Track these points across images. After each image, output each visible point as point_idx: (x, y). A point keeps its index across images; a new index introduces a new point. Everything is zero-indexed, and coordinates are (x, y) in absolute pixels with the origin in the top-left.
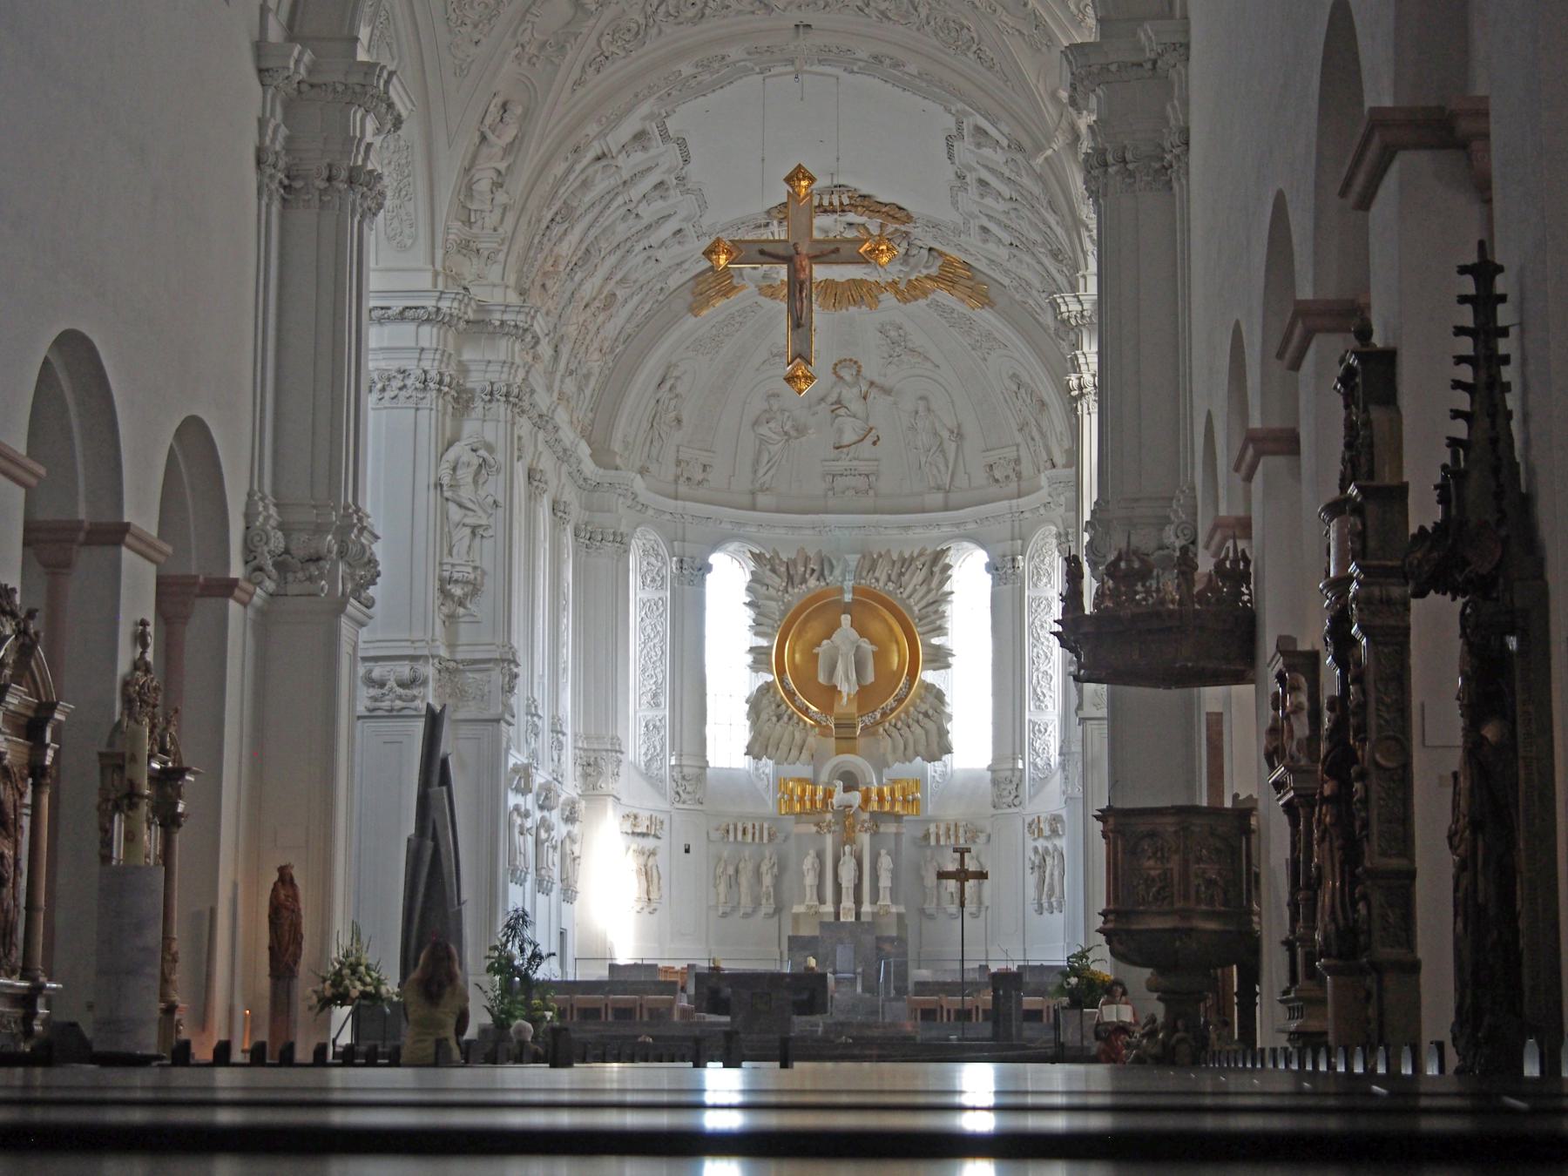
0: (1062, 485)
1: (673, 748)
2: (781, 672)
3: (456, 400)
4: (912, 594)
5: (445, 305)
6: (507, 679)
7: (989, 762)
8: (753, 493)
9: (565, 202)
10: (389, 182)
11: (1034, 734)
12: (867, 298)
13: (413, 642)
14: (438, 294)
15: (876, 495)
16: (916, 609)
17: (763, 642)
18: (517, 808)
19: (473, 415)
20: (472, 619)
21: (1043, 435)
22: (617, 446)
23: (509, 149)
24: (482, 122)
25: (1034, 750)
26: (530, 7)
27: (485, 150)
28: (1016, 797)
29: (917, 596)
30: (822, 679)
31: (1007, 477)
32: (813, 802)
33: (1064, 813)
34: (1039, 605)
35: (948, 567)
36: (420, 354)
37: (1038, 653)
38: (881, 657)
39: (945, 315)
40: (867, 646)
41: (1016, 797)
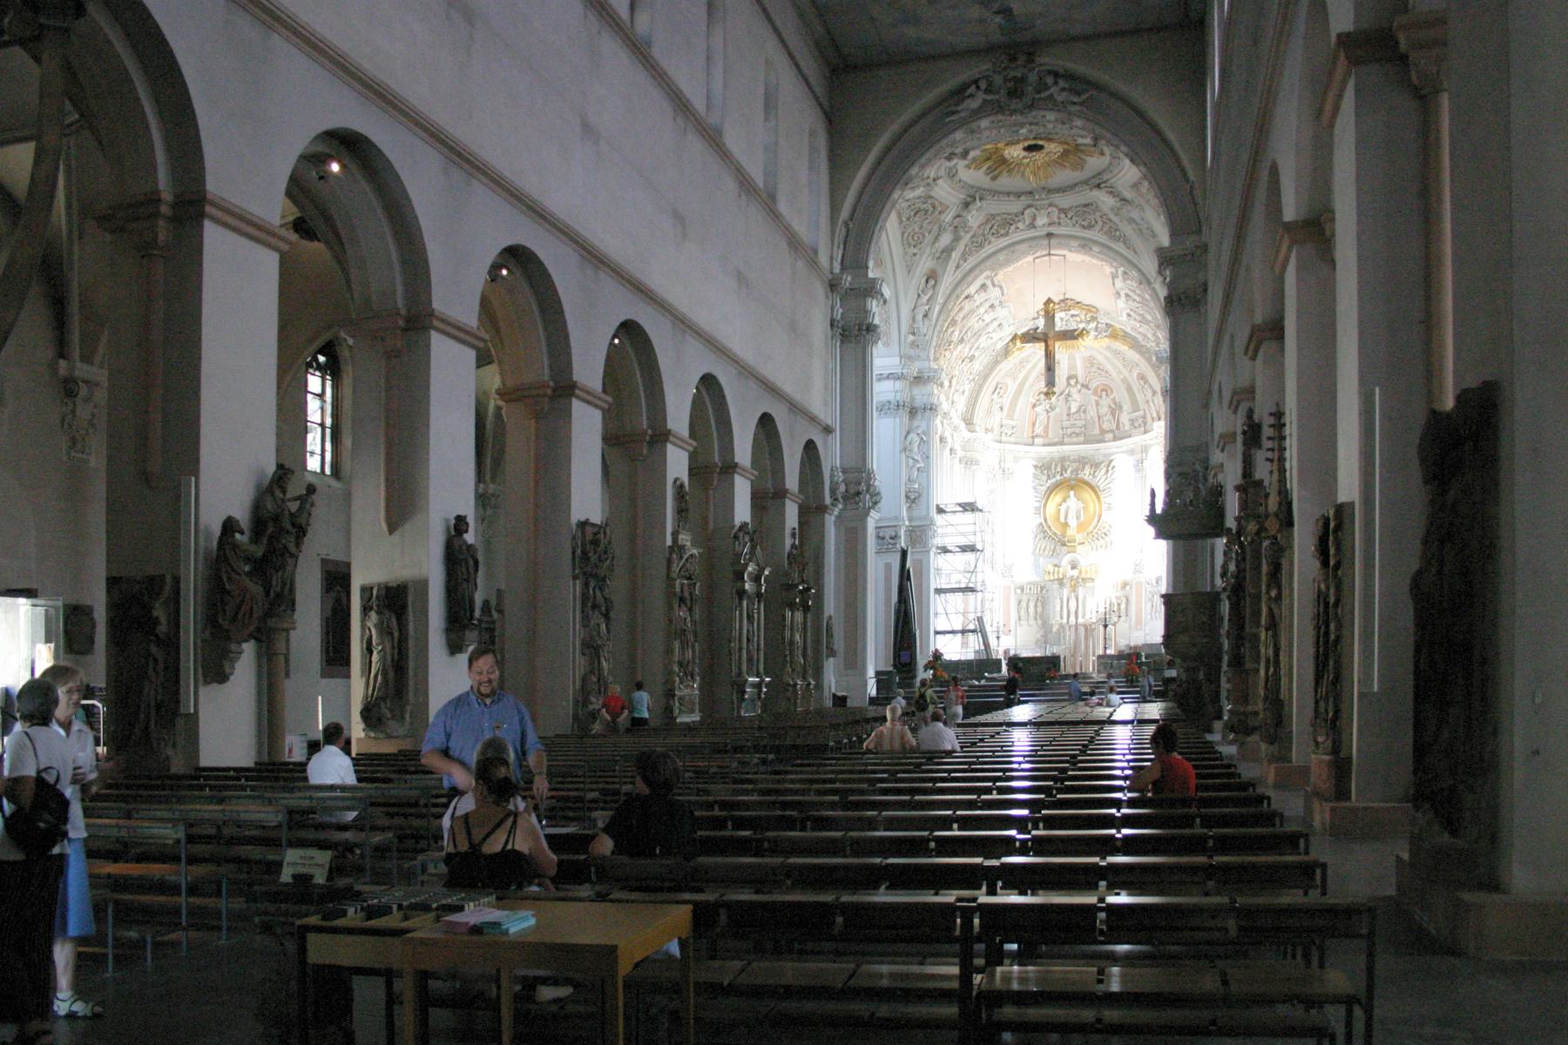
8: (1033, 437)
10: (882, 328)
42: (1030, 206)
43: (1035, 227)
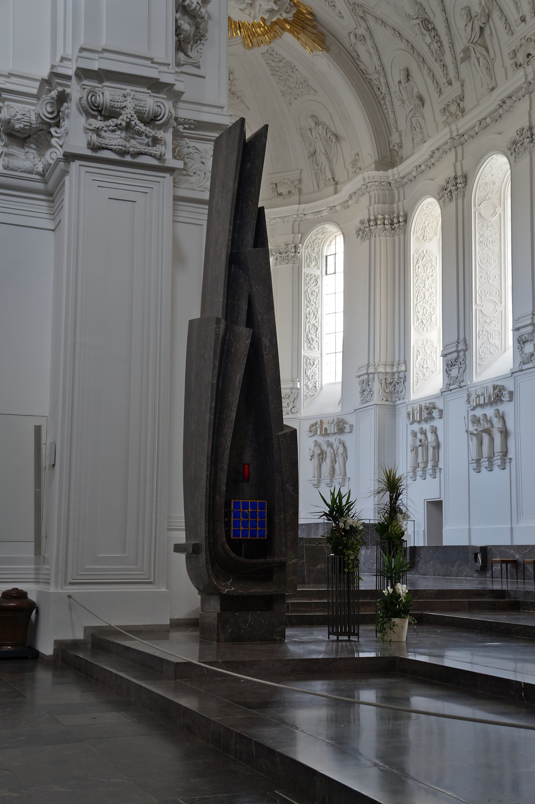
0: (377, 184)
11: (307, 365)
25: (307, 376)
28: (293, 407)
31: (290, 192)
34: (310, 280)
37: (309, 311)
39: (273, 64)
41: (293, 407)
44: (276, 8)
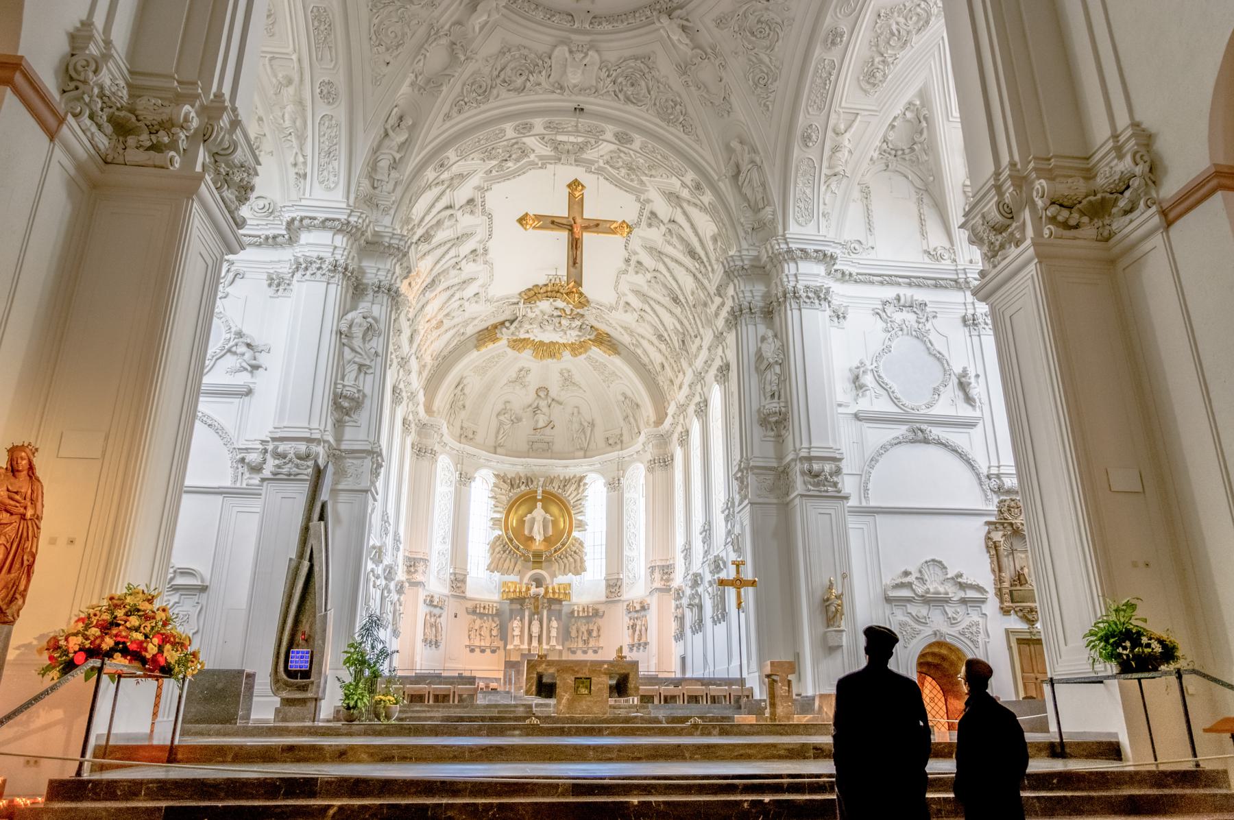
1: (451, 564)
2: (507, 529)
3: (356, 288)
4: (570, 495)
5: (353, 219)
6: (375, 466)
7: (604, 575)
8: (495, 447)
9: (427, 231)
12: (557, 355)
13: (310, 429)
14: (349, 211)
15: (552, 452)
16: (572, 502)
17: (498, 516)
18: (372, 571)
19: (367, 299)
20: (354, 424)
21: (636, 420)
22: (435, 408)
23: (402, 146)
24: (386, 121)
26: (424, 44)
27: (387, 142)
29: (573, 496)
30: (526, 532)
32: (520, 592)
33: (648, 600)
35: (585, 484)
36: (334, 250)
38: (555, 523)
40: (548, 516)
42: (563, 42)
43: (561, 88)
44: (580, 334)
